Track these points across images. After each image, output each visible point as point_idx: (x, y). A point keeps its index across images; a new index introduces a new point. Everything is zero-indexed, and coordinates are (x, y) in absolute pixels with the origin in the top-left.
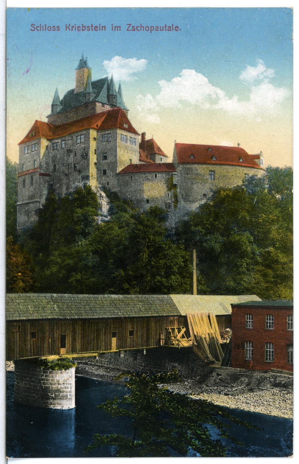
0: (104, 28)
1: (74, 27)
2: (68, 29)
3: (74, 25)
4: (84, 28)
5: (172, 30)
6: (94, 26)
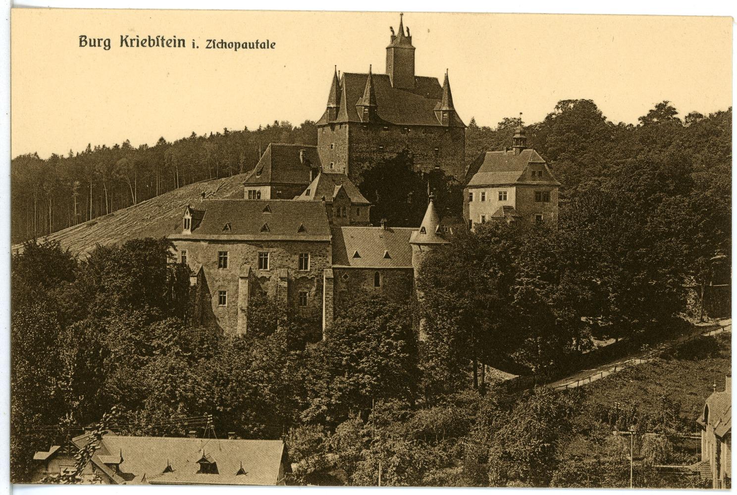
0: (182, 42)
1: (134, 40)
2: (124, 42)
3: (136, 38)
4: (152, 42)
5: (266, 46)
6: (166, 38)
